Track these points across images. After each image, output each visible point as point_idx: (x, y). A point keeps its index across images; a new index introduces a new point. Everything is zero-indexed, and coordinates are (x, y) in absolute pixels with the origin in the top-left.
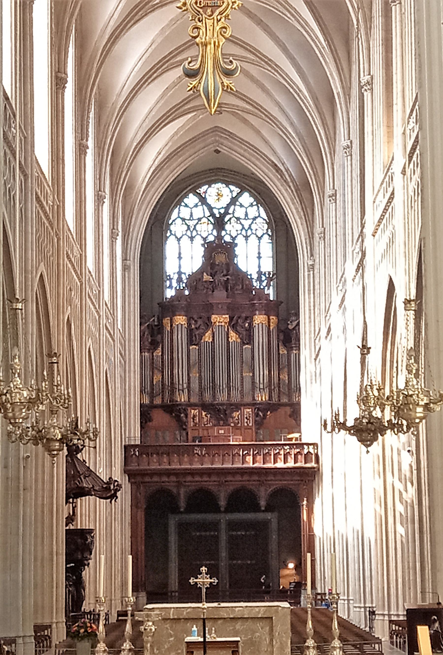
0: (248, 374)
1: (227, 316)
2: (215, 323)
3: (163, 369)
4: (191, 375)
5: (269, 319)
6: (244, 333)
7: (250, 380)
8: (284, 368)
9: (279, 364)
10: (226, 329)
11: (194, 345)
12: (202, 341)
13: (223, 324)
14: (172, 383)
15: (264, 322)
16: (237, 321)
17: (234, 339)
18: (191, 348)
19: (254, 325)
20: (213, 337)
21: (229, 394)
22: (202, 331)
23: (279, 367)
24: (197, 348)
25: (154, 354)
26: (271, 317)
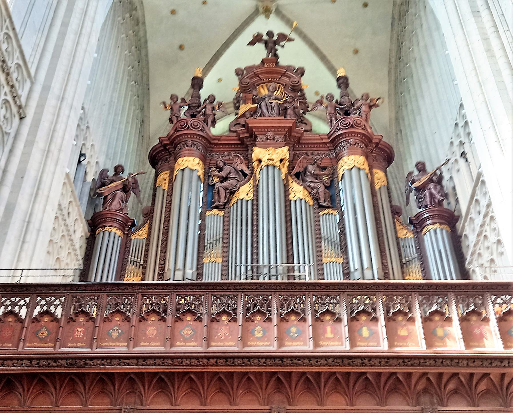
1: (286, 148)
2: (260, 161)
3: (145, 262)
4: (206, 260)
5: (371, 173)
8: (408, 262)
10: (283, 176)
11: (217, 207)
12: (233, 201)
13: (278, 164)
15: (362, 167)
16: (306, 169)
17: (300, 195)
18: (208, 213)
19: (341, 172)
22: (233, 182)
24: (222, 213)
25: (133, 237)
26: (375, 171)
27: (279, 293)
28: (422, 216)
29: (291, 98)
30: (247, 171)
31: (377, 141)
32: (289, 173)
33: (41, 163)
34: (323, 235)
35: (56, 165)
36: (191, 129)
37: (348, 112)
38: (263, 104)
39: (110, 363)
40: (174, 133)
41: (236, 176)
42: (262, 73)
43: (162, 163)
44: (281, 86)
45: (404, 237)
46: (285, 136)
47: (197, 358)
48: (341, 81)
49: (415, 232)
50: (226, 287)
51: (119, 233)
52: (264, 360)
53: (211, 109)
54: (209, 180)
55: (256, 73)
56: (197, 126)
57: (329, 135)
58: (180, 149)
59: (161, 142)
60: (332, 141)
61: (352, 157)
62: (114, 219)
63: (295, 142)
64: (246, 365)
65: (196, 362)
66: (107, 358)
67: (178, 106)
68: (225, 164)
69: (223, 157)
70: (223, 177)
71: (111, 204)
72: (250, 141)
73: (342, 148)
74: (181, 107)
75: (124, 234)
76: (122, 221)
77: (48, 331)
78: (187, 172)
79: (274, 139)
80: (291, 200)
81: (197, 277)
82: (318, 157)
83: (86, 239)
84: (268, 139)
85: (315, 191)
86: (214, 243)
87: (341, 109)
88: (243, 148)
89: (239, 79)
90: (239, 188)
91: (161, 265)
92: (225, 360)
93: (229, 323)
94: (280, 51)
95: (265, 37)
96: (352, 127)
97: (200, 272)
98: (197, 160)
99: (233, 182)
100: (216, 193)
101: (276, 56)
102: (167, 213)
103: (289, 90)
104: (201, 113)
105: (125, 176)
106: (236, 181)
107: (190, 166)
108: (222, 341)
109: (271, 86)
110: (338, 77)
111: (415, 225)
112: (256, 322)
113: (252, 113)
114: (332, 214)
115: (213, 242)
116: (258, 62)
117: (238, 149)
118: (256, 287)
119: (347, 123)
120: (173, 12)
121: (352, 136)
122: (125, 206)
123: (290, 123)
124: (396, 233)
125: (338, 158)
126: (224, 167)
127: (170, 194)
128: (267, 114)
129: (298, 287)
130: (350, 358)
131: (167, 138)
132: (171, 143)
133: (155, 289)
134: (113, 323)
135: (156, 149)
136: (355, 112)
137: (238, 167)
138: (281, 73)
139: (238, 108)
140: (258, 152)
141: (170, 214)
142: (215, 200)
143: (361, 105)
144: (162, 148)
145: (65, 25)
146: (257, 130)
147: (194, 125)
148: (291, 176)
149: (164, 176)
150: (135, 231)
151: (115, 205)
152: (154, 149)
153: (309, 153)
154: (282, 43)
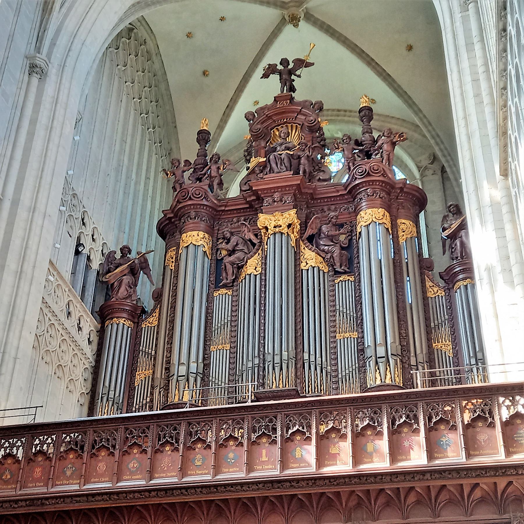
0: (347, 335)
2: (267, 228)
6: (336, 251)
7: (353, 347)
9: (427, 319)
11: (225, 286)
13: (285, 230)
14: (168, 369)
16: (320, 230)
17: (312, 263)
18: (215, 294)
19: (359, 230)
20: (265, 264)
21: (299, 376)
23: (427, 326)
24: (230, 293)
26: (399, 221)
27: (220, 418)
28: (452, 271)
29: (303, 145)
30: (255, 241)
31: (401, 185)
32: (301, 237)
33: (14, 287)
34: (338, 308)
35: (31, 284)
36: (193, 199)
37: (370, 153)
38: (272, 157)
39: (64, 501)
40: (176, 205)
41: (243, 248)
42: (276, 114)
43: (169, 238)
44: (299, 126)
45: (434, 296)
46: (295, 195)
47: (139, 492)
48: (362, 113)
49: (447, 289)
50: (170, 417)
51: (128, 323)
52: (200, 489)
53: (216, 170)
54: (217, 254)
55: (268, 115)
56: (199, 194)
57: (346, 186)
58: (183, 223)
59: (165, 215)
60: (350, 192)
61: (369, 211)
62: (121, 309)
63: (308, 198)
64: (186, 495)
65: (139, 496)
66: (60, 497)
67: (180, 171)
68: (232, 234)
69: (232, 224)
70: (230, 250)
71: (118, 291)
72: (258, 204)
73: (359, 200)
74: (184, 171)
75: (134, 323)
76: (129, 310)
77: (11, 473)
78: (191, 249)
79: (281, 201)
80: (302, 270)
81: (204, 368)
82: (332, 214)
83: (97, 332)
84: (275, 202)
85: (329, 255)
86: (222, 328)
87: (361, 151)
88: (253, 211)
89: (250, 125)
90: (247, 262)
91: (168, 358)
92: (165, 492)
93: (173, 453)
94: (297, 83)
95: (280, 67)
96: (369, 175)
97: (207, 362)
98: (201, 234)
99: (239, 254)
100: (224, 269)
101: (292, 89)
102: (173, 298)
103: (306, 131)
104: (206, 176)
105: (133, 255)
106: (244, 253)
107: (194, 243)
108: (164, 472)
109: (283, 132)
110: (361, 106)
111: (446, 280)
112: (197, 450)
113: (261, 168)
114: (349, 280)
115: (215, 331)
116: (270, 101)
117: (247, 214)
118: (197, 414)
119: (363, 171)
120: (189, 35)
121: (369, 185)
122: (134, 291)
123: (297, 180)
124: (424, 291)
125: (356, 212)
126: (232, 237)
127: (177, 277)
128: (276, 170)
129: (237, 411)
130: (279, 482)
131: (170, 211)
132: (176, 216)
133: (105, 424)
134: (67, 461)
135: (162, 223)
136: (377, 152)
137: (246, 236)
138: (297, 112)
139: (248, 161)
140: (263, 219)
141: (176, 299)
142: (223, 277)
143: (383, 143)
144: (167, 222)
145: (33, 122)
146: (262, 192)
147: (196, 194)
148: (303, 241)
149: (172, 253)
150: (146, 318)
151: (123, 292)
152: (160, 223)
153: (326, 208)
154: (298, 73)
